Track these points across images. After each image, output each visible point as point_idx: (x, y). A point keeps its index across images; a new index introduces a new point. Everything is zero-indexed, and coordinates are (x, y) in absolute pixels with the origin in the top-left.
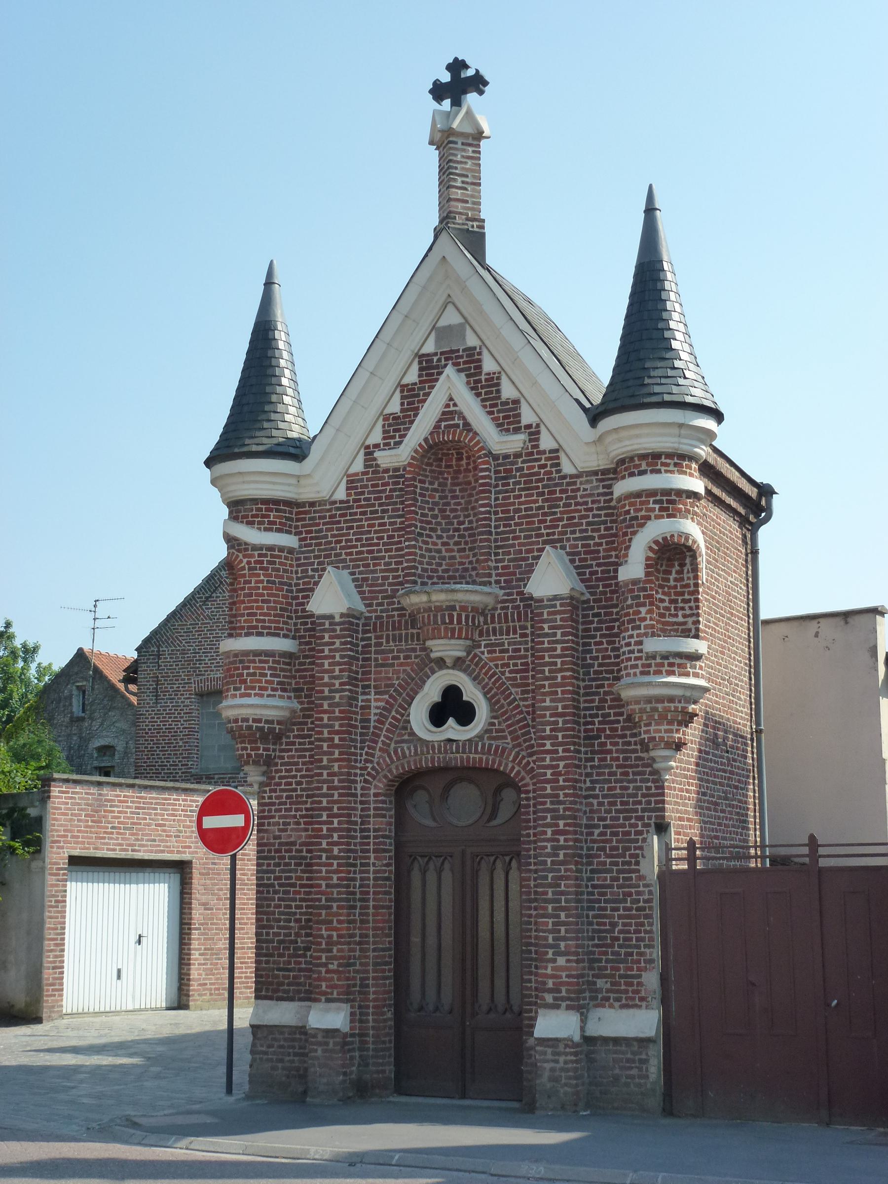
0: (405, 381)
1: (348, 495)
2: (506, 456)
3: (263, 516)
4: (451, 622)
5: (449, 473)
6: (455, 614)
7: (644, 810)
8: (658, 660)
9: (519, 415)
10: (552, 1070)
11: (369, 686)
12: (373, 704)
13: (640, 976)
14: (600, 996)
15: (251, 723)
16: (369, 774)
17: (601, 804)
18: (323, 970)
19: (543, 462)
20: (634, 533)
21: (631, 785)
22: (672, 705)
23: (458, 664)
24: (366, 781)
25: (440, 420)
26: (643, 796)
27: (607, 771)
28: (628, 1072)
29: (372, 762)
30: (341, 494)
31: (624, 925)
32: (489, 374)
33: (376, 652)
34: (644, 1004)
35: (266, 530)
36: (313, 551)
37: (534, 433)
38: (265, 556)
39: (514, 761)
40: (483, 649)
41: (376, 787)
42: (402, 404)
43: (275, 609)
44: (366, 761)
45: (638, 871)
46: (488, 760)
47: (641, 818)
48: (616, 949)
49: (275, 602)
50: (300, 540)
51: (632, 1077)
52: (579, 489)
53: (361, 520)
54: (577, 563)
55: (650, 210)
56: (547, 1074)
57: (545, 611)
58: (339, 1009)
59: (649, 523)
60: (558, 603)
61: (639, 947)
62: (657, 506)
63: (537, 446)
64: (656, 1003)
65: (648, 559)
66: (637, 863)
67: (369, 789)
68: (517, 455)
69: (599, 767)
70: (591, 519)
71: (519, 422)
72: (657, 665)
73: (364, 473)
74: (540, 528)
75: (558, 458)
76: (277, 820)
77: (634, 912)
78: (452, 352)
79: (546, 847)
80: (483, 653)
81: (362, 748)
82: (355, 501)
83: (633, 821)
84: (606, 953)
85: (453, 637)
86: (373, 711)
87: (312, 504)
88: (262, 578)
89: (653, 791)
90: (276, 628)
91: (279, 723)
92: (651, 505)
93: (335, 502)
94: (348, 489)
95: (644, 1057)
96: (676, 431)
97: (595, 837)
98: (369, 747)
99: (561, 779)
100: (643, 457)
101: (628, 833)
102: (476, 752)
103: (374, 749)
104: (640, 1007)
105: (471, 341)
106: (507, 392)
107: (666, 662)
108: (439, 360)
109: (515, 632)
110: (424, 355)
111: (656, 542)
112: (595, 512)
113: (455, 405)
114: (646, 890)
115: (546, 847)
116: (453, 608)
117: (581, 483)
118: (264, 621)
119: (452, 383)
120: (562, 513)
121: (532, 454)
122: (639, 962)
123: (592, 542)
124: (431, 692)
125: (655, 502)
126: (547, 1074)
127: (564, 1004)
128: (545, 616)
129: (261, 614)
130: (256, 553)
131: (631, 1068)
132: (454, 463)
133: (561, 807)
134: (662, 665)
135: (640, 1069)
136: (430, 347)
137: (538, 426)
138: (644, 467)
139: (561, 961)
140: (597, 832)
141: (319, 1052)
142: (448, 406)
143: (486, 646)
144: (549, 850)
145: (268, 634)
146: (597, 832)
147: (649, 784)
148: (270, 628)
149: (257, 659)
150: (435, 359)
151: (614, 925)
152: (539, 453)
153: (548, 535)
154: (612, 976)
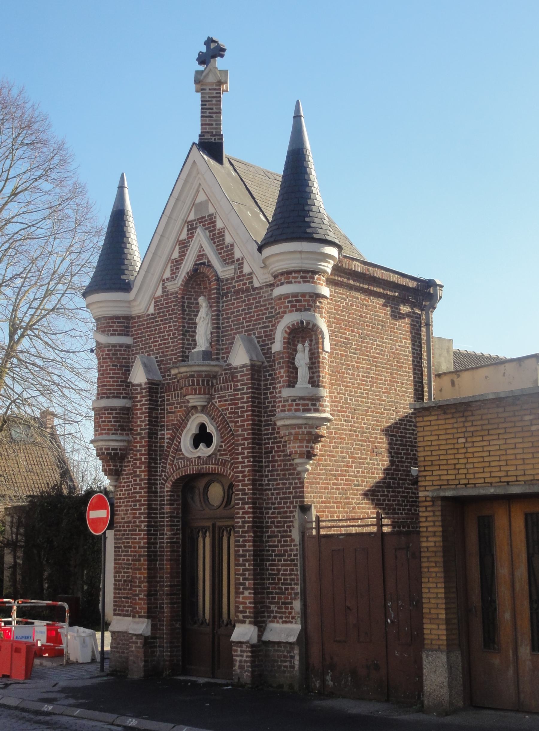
0: (181, 239)
1: (155, 310)
2: (227, 280)
3: (110, 327)
4: (193, 385)
5: (206, 292)
6: (195, 379)
7: (294, 497)
8: (290, 402)
9: (233, 254)
10: (241, 661)
11: (163, 426)
12: (166, 436)
13: (291, 603)
14: (272, 615)
15: (104, 451)
16: (163, 479)
17: (272, 494)
18: (137, 598)
19: (245, 281)
20: (278, 322)
21: (287, 482)
22: (300, 430)
23: (204, 409)
24: (162, 484)
25: (197, 260)
26: (294, 488)
27: (275, 473)
28: (284, 664)
29: (165, 472)
30: (151, 310)
31: (284, 570)
32: (219, 230)
33: (168, 405)
34: (294, 621)
35: (112, 335)
36: (139, 345)
37: (240, 263)
38: (111, 350)
39: (230, 469)
40: (216, 400)
41: (167, 487)
42: (179, 252)
43: (117, 382)
44: (162, 471)
45: (290, 536)
46: (218, 469)
47: (292, 503)
48: (280, 586)
49: (117, 378)
50: (134, 339)
51: (286, 667)
52: (261, 297)
53: (160, 325)
54: (261, 343)
55: (297, 117)
56: (238, 664)
57: (239, 375)
58: (143, 622)
59: (286, 315)
60: (245, 369)
61: (291, 584)
62: (289, 305)
63: (241, 272)
64: (299, 620)
65: (284, 338)
66: (290, 531)
67: (164, 488)
68: (233, 279)
69: (272, 471)
70: (268, 315)
71: (233, 258)
72: (289, 405)
73: (162, 296)
74: (243, 323)
75: (252, 278)
76: (123, 508)
77: (289, 562)
78: (203, 218)
79: (239, 522)
80: (216, 402)
81: (160, 464)
82: (159, 313)
83: (288, 504)
84: (275, 588)
85: (195, 394)
86: (166, 441)
87: (139, 317)
88: (109, 363)
89: (298, 485)
90: (117, 393)
91: (120, 450)
92: (286, 304)
93: (148, 315)
94: (155, 306)
95: (292, 654)
96: (298, 256)
97: (270, 515)
98: (163, 463)
99: (246, 479)
100: (282, 274)
101: (285, 512)
102: (212, 464)
103: (166, 463)
104: (291, 622)
105: (211, 210)
106: (228, 240)
107: (294, 403)
108: (196, 224)
109: (231, 389)
110: (189, 222)
111: (289, 327)
112: (270, 310)
113: (203, 250)
114: (295, 548)
115: (239, 522)
116: (193, 376)
117: (263, 293)
118: (110, 389)
119: (201, 238)
120: (254, 312)
121: (239, 277)
122: (291, 594)
123: (268, 329)
124: (192, 428)
125: (289, 302)
126: (238, 664)
127: (248, 620)
128: (239, 378)
129: (109, 386)
130: (106, 349)
131: (286, 662)
132: (208, 286)
133: (246, 497)
134: (292, 405)
135: (291, 662)
136: (192, 217)
137: (242, 259)
138: (283, 280)
139: (247, 593)
140: (271, 511)
141: (133, 649)
142: (200, 251)
143: (218, 398)
144: (240, 524)
145: (113, 397)
146: (271, 511)
147: (296, 481)
148: (114, 393)
149: (106, 412)
150: (195, 223)
151: (279, 570)
152: (244, 276)
153: (247, 326)
154: (277, 603)
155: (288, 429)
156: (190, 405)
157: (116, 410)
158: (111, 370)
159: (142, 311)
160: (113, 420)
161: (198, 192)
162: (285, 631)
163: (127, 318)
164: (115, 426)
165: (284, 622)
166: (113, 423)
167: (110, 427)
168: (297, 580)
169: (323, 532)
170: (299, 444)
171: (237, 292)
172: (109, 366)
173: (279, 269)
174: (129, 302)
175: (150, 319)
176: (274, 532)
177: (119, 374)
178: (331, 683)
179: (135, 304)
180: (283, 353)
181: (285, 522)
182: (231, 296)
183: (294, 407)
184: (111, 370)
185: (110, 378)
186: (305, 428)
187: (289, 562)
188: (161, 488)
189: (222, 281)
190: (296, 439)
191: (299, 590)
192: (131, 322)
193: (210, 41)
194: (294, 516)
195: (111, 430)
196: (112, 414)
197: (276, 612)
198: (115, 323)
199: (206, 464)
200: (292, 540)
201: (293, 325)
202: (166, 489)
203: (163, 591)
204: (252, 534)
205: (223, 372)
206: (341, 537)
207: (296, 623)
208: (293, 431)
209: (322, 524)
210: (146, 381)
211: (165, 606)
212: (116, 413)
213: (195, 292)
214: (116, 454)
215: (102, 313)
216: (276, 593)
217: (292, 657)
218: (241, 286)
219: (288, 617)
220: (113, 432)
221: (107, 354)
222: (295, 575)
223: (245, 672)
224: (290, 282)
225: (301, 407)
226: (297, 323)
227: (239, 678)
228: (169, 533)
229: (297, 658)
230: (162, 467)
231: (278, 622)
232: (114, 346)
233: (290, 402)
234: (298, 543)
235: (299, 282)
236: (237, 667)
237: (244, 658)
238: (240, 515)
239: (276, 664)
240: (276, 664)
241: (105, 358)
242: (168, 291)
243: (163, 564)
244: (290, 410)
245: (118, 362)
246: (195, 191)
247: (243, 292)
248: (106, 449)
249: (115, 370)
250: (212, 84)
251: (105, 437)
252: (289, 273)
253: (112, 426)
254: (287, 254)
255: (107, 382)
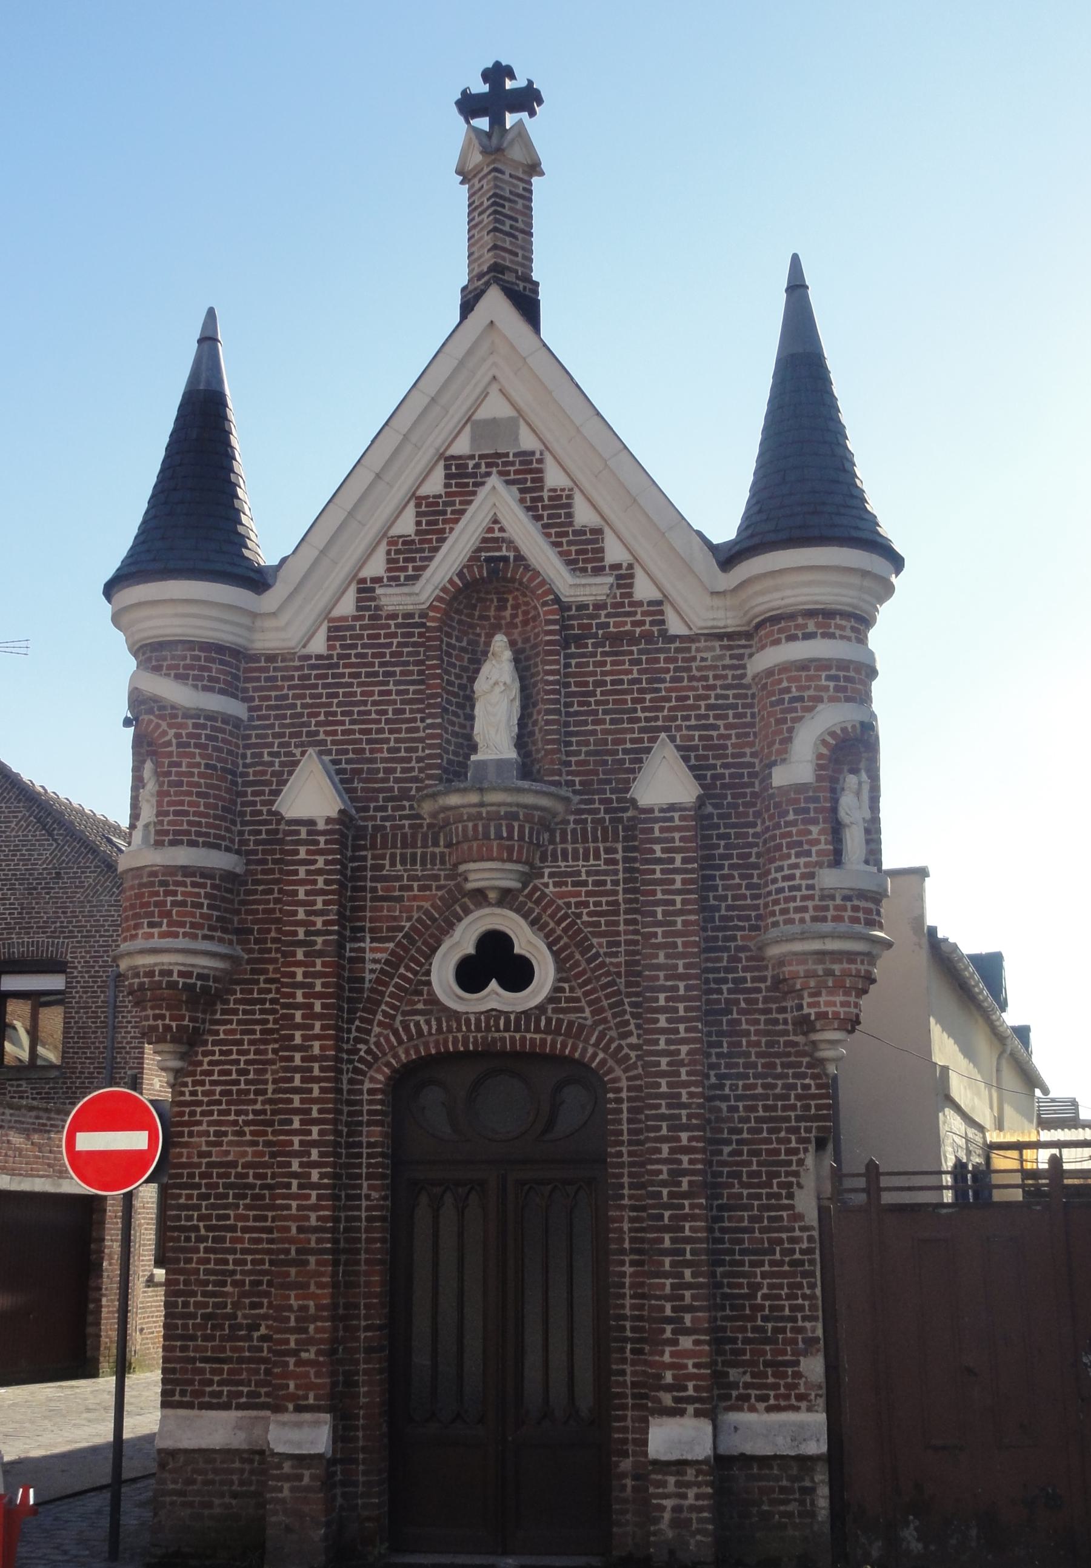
0: (423, 491)
1: (330, 648)
2: (582, 607)
3: (202, 668)
4: (510, 837)
5: (483, 627)
6: (516, 825)
7: (798, 1119)
8: (838, 902)
9: (601, 550)
10: (677, 1509)
11: (362, 929)
12: (368, 956)
13: (797, 1363)
14: (734, 1393)
15: (175, 977)
16: (362, 1060)
17: (733, 1109)
18: (292, 1361)
19: (639, 617)
20: (799, 719)
21: (780, 1082)
22: (853, 966)
23: (506, 898)
24: (356, 1070)
25: (479, 550)
26: (798, 1097)
27: (741, 1061)
28: (782, 1508)
29: (366, 1042)
30: (318, 645)
31: (771, 1286)
32: (551, 490)
33: (374, 879)
34: (803, 1405)
35: (206, 689)
36: (272, 726)
37: (624, 577)
38: (204, 727)
39: (596, 1045)
40: (546, 880)
41: (373, 1080)
42: (418, 523)
43: (215, 807)
44: (357, 1040)
45: (791, 1207)
46: (559, 1044)
47: (795, 1130)
48: (759, 1323)
49: (216, 797)
50: (250, 709)
51: (789, 1515)
52: (694, 659)
53: (351, 685)
54: (693, 762)
55: (797, 288)
56: (667, 1516)
57: (657, 827)
58: (317, 1423)
59: (821, 707)
60: (676, 815)
61: (794, 1320)
62: (832, 684)
63: (630, 595)
64: (821, 1402)
65: (820, 756)
66: (790, 1196)
67: (362, 1083)
68: (599, 606)
69: (730, 1055)
70: (712, 701)
71: (602, 559)
72: (837, 908)
73: (356, 618)
74: (635, 710)
75: (662, 613)
76: (204, 1127)
77: (786, 1268)
78: (498, 455)
79: (660, 1172)
80: (546, 885)
81: (351, 1021)
82: (341, 657)
83: (783, 1134)
84: (744, 1329)
85: (510, 860)
86: (369, 966)
87: (271, 658)
88: (198, 759)
89: (813, 1090)
90: (216, 836)
91: (216, 980)
92: (824, 682)
93: (308, 657)
94: (329, 639)
95: (807, 1483)
96: (855, 580)
97: (725, 1157)
98: (363, 1020)
99: (683, 1070)
100: (810, 614)
101: (777, 1152)
102: (537, 1030)
103: (370, 1022)
104: (797, 1409)
105: (527, 442)
106: (583, 516)
107: (849, 904)
108: (477, 466)
109: (597, 857)
110: (453, 457)
111: (833, 734)
112: (719, 691)
113: (502, 530)
114: (805, 1235)
115: (660, 1172)
116: (514, 816)
117: (698, 650)
118: (199, 824)
119: (497, 502)
120: (668, 690)
121: (622, 605)
122: (794, 1342)
123: (714, 733)
124: (463, 941)
125: (829, 678)
126: (667, 1516)
127: (691, 1409)
128: (657, 834)
129: (195, 814)
130: (190, 722)
131: (786, 1502)
132: (492, 613)
133: (684, 1112)
134: (844, 908)
135: (802, 1502)
136: (462, 447)
137: (630, 566)
138: (811, 627)
139: (686, 1343)
140: (727, 1149)
141: (286, 1493)
142: (490, 530)
143: (552, 875)
144: (664, 1176)
145: (206, 845)
146: (727, 1149)
147: (807, 1081)
148: (207, 835)
149: (188, 880)
150: (471, 463)
151: (755, 1287)
152: (632, 604)
153: (647, 719)
154: (753, 1363)
155: (822, 962)
156: (470, 886)
157: (211, 877)
158: (201, 775)
159: (292, 644)
160: (206, 902)
161: (485, 394)
162: (789, 1429)
163: (237, 653)
164: (209, 917)
165: (769, 1409)
166: (205, 910)
167: (198, 920)
168: (813, 1307)
169: (887, 1198)
170: (842, 998)
171: (617, 639)
172: (198, 765)
173: (805, 603)
174: (254, 615)
175: (313, 667)
176: (740, 1196)
177: (219, 788)
178: (916, 1547)
179: (270, 623)
180: (816, 789)
181: (772, 1175)
182: (595, 645)
183: (849, 913)
184: (201, 775)
185: (199, 795)
186: (862, 963)
187: (786, 1268)
188: (351, 1081)
189: (569, 609)
190: (839, 985)
191: (819, 1333)
192: (243, 665)
193: (497, 73)
194: (801, 1162)
195: (200, 926)
196: (203, 886)
197: (747, 1386)
198: (213, 661)
199: (517, 1029)
200: (800, 1217)
201: (844, 730)
202: (367, 1085)
203: (357, 1339)
204: (703, 1201)
205: (572, 818)
206: (944, 1211)
207: (809, 1409)
208: (837, 968)
209: (884, 1182)
210: (334, 814)
211: (361, 1378)
212: (213, 887)
213: (460, 622)
214: (205, 989)
215: (179, 631)
216: (747, 1341)
217: (812, 1490)
218: (628, 627)
219: (787, 1397)
220: (206, 932)
221: (190, 735)
222: (805, 1297)
223: (693, 1534)
224: (832, 636)
225: (861, 915)
226: (854, 727)
227: (672, 1552)
228: (375, 1195)
229: (824, 1491)
230: (358, 1029)
231: (752, 1409)
232: (211, 717)
233: (838, 902)
234: (815, 1224)
235: (849, 639)
236: (664, 1525)
237: (691, 1500)
238: (665, 1154)
239: (755, 1510)
240: (755, 1510)
241: (188, 745)
242: (377, 608)
243: (357, 1274)
244: (837, 919)
245: (219, 759)
246: (478, 390)
247: (633, 640)
248: (181, 974)
249: (211, 777)
250: (517, 164)
251: (182, 943)
252: (828, 614)
253: (202, 915)
254: (800, 574)
255: (190, 804)
